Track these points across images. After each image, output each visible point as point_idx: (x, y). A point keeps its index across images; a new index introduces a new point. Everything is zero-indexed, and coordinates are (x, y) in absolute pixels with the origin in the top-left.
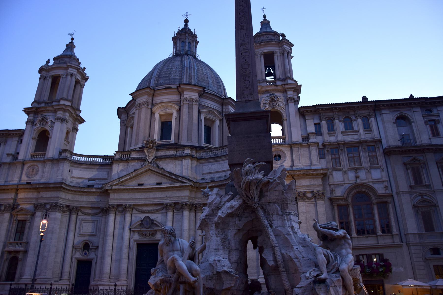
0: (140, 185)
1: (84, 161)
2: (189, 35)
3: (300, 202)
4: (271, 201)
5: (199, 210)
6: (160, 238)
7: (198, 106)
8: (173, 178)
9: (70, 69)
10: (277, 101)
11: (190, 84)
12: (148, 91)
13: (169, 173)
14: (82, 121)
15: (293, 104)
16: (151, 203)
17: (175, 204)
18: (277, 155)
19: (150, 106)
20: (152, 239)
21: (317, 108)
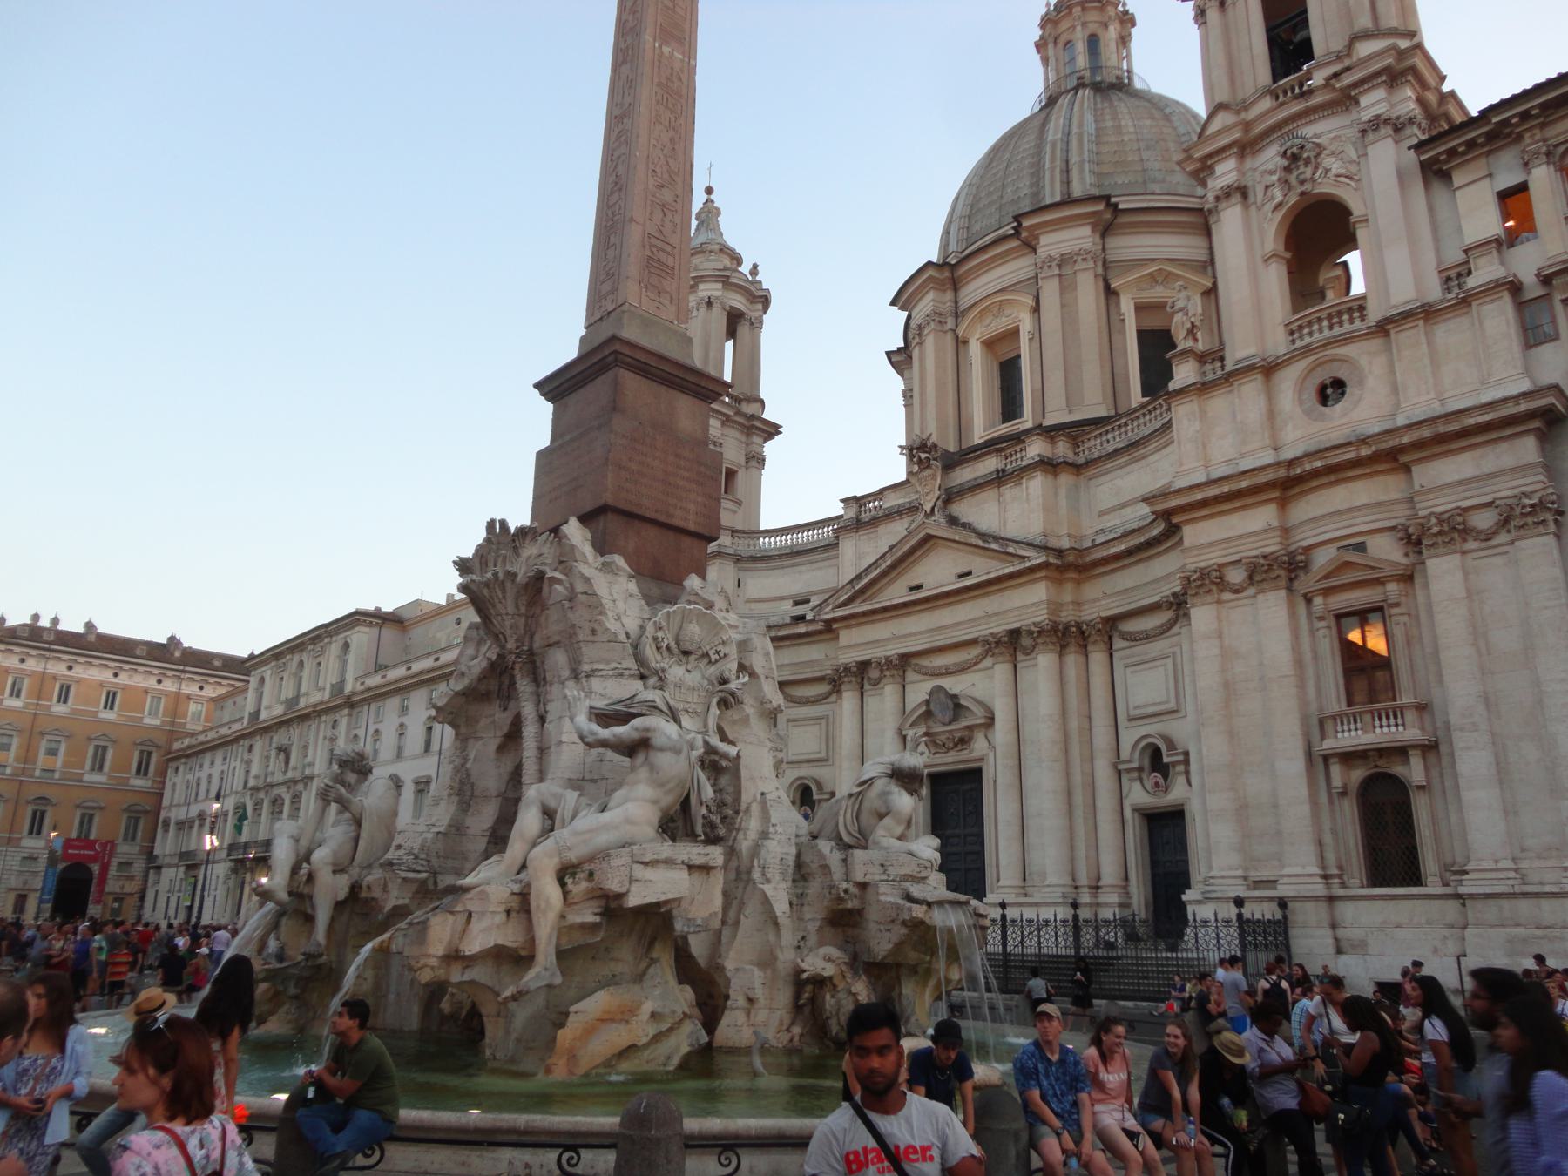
0: (912, 589)
1: (775, 549)
2: (1084, 9)
3: (1437, 556)
4: (551, 641)
5: (1095, 642)
6: (984, 752)
7: (1100, 270)
8: (996, 551)
9: (701, 287)
10: (1318, 155)
11: (1067, 201)
12: (930, 277)
13: (982, 536)
14: (772, 430)
15: (1389, 141)
16: (948, 642)
17: (1015, 634)
18: (1328, 382)
19: (950, 323)
20: (964, 755)
21: (1495, 120)
